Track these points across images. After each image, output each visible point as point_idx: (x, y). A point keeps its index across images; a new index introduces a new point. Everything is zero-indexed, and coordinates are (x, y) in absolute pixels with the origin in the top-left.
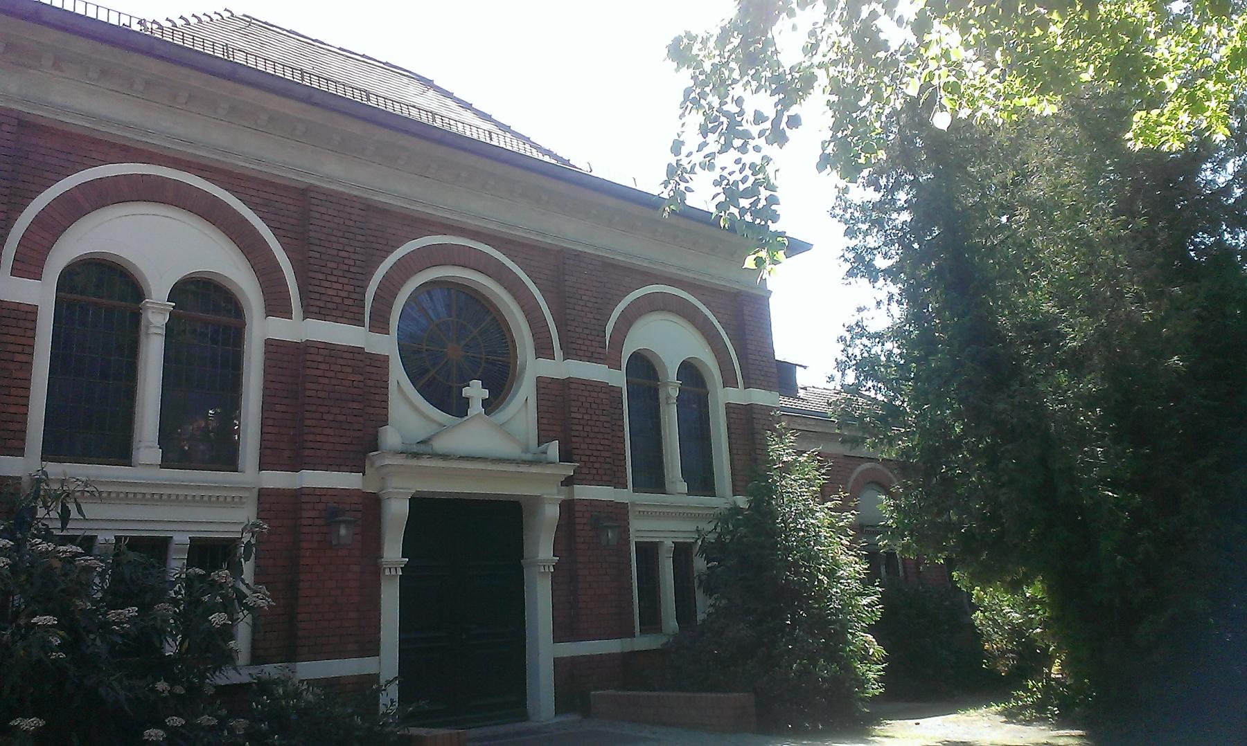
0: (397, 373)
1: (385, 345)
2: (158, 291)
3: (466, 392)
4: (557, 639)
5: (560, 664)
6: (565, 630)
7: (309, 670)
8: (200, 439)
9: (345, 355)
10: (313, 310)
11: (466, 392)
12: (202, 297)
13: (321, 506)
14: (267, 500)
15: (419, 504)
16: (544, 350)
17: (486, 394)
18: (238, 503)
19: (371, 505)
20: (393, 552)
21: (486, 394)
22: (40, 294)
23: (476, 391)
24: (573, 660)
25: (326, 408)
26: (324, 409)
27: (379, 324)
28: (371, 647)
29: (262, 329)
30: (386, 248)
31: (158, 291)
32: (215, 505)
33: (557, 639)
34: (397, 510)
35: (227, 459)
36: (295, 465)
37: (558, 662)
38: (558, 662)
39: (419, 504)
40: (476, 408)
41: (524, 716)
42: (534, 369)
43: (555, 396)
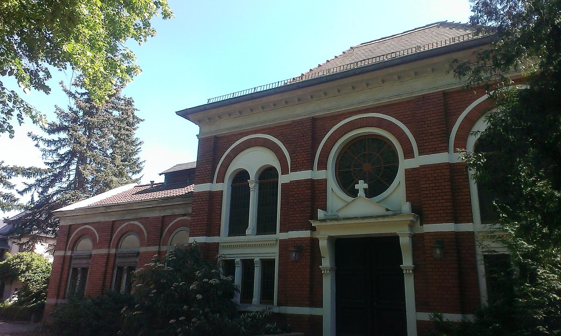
1: (328, 175)
3: (357, 186)
6: (420, 306)
11: (357, 186)
12: (267, 175)
14: (284, 245)
16: (409, 154)
17: (366, 186)
18: (272, 245)
19: (314, 242)
20: (326, 263)
21: (366, 186)
22: (224, 187)
23: (361, 186)
29: (283, 179)
40: (361, 193)
42: (404, 164)
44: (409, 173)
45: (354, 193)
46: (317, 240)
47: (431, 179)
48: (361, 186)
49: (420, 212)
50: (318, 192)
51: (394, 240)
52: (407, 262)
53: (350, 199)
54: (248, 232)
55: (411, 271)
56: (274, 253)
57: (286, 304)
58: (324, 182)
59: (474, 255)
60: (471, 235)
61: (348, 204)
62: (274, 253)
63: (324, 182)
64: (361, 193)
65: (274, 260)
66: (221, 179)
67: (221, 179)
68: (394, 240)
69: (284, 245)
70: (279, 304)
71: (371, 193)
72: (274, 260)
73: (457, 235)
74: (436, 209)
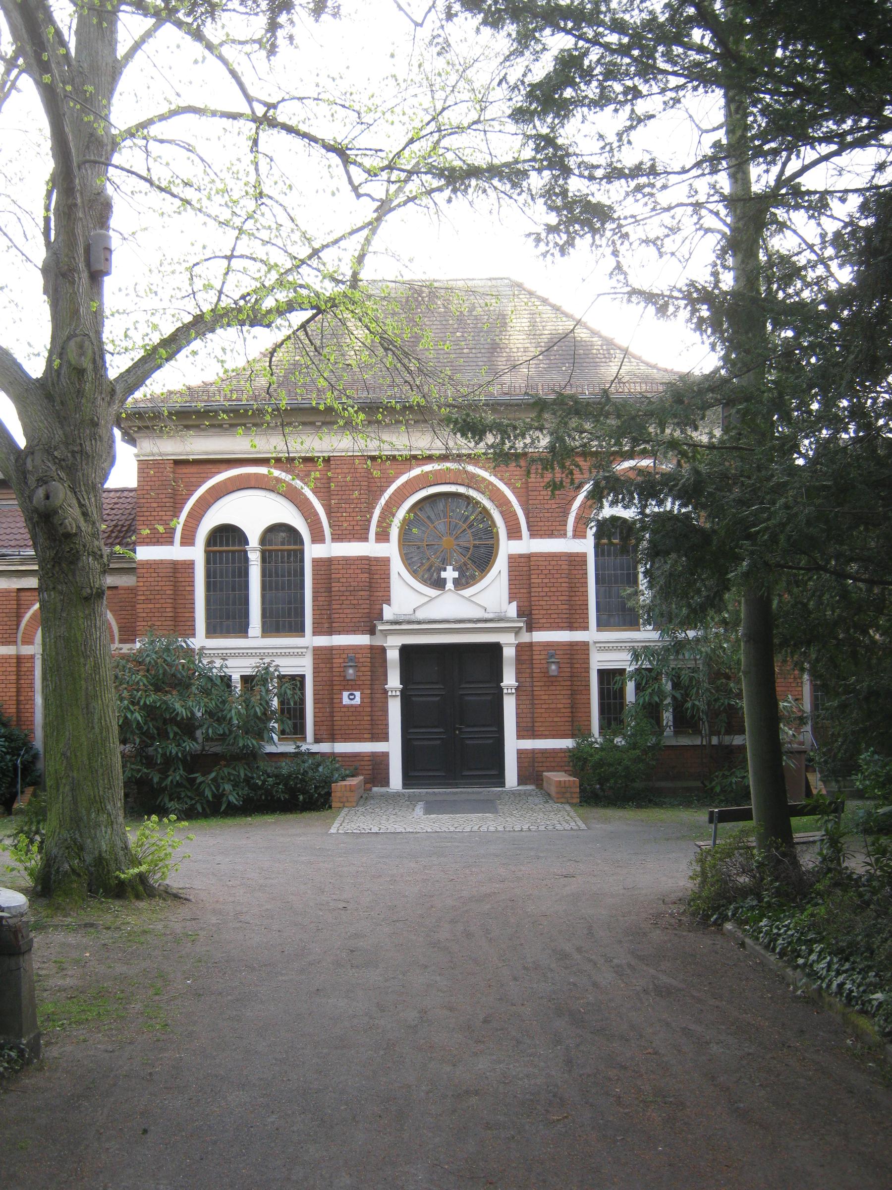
0: (397, 567)
1: (390, 550)
2: (254, 541)
3: (443, 575)
4: (519, 737)
5: (521, 754)
7: (342, 747)
8: (283, 619)
9: (356, 562)
10: (338, 537)
11: (443, 575)
13: (344, 656)
15: (406, 651)
16: (514, 533)
17: (456, 574)
18: (302, 655)
20: (394, 681)
21: (456, 574)
22: (196, 554)
23: (450, 574)
24: (533, 751)
25: (357, 594)
26: (344, 598)
27: (383, 536)
28: (385, 738)
29: (313, 551)
30: (385, 484)
31: (254, 541)
32: (295, 655)
33: (519, 737)
34: (393, 655)
35: (298, 629)
36: (330, 632)
37: (521, 753)
38: (521, 753)
39: (406, 651)
40: (450, 585)
41: (503, 784)
42: (507, 548)
43: (523, 570)
44: (515, 561)
45: (439, 584)
46: (383, 650)
47: (544, 572)
48: (450, 574)
49: (530, 618)
50: (376, 576)
51: (496, 649)
52: (509, 679)
53: (433, 592)
54: (251, 632)
55: (514, 691)
56: (304, 666)
57: (333, 739)
58: (385, 562)
59: (587, 670)
60: (585, 645)
61: (432, 599)
62: (304, 666)
63: (386, 561)
64: (450, 585)
65: (303, 677)
66: (188, 540)
67: (188, 540)
68: (496, 649)
69: (322, 656)
70: (317, 741)
71: (459, 584)
72: (303, 677)
73: (572, 645)
74: (549, 612)
